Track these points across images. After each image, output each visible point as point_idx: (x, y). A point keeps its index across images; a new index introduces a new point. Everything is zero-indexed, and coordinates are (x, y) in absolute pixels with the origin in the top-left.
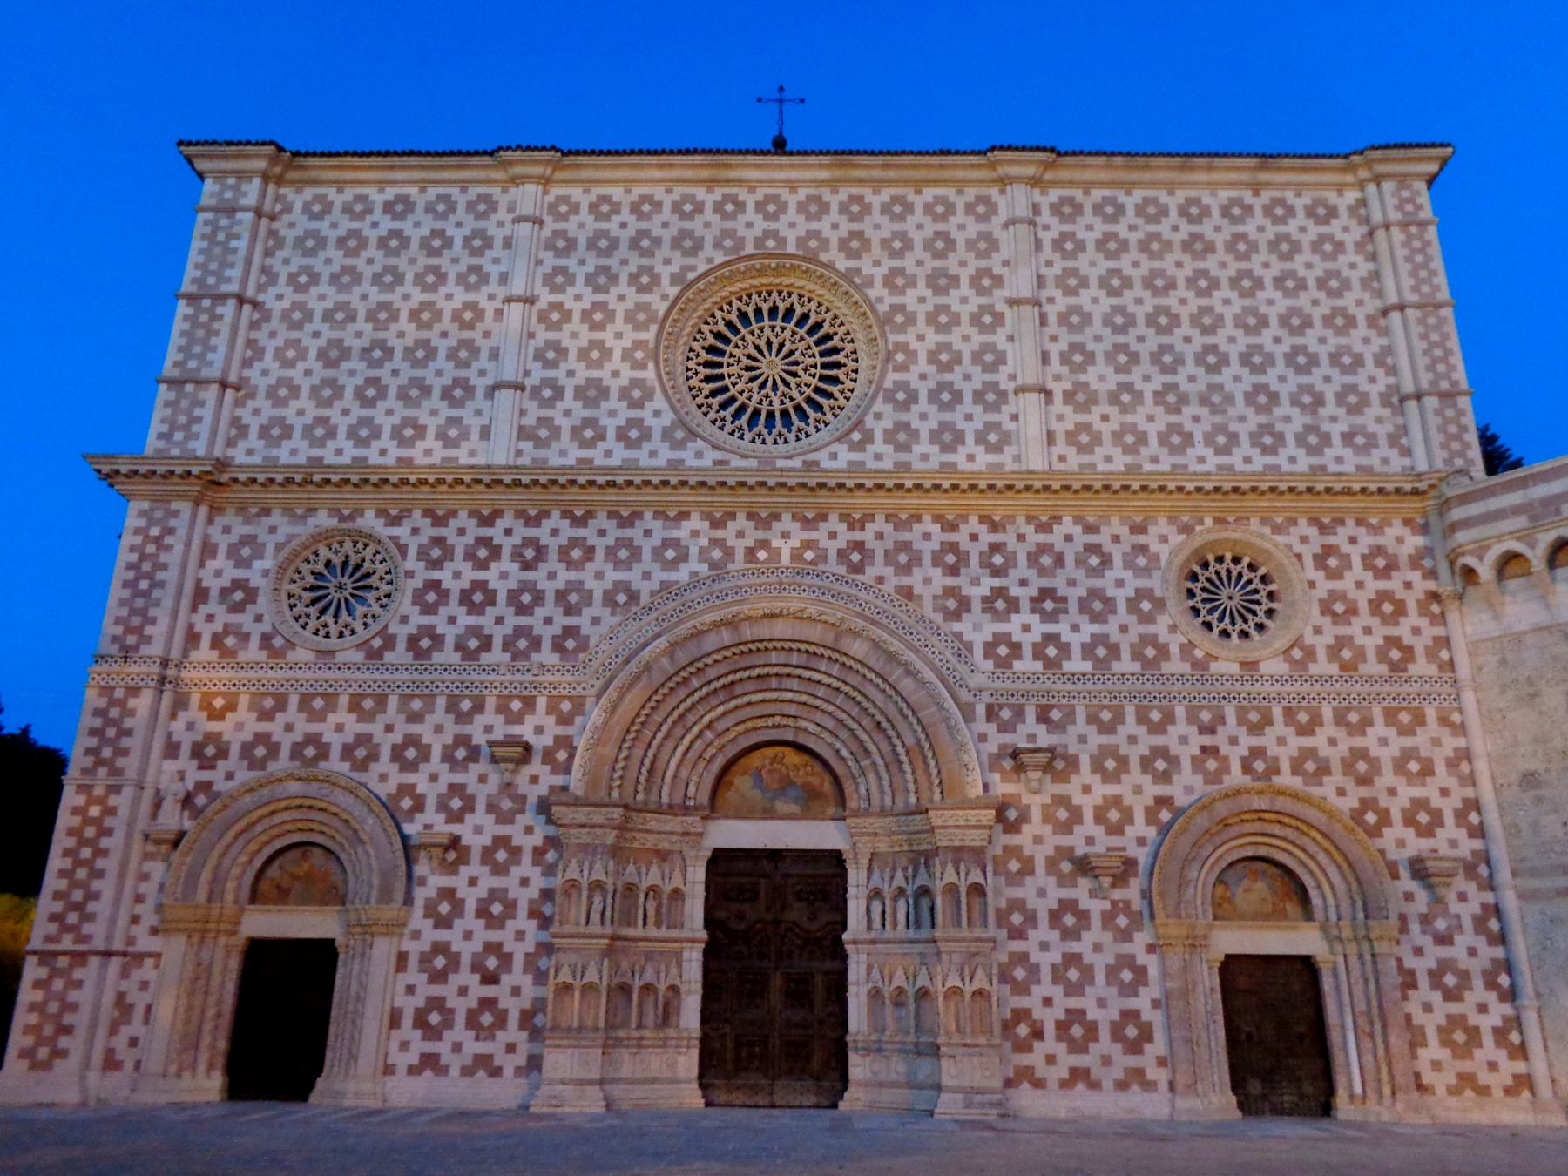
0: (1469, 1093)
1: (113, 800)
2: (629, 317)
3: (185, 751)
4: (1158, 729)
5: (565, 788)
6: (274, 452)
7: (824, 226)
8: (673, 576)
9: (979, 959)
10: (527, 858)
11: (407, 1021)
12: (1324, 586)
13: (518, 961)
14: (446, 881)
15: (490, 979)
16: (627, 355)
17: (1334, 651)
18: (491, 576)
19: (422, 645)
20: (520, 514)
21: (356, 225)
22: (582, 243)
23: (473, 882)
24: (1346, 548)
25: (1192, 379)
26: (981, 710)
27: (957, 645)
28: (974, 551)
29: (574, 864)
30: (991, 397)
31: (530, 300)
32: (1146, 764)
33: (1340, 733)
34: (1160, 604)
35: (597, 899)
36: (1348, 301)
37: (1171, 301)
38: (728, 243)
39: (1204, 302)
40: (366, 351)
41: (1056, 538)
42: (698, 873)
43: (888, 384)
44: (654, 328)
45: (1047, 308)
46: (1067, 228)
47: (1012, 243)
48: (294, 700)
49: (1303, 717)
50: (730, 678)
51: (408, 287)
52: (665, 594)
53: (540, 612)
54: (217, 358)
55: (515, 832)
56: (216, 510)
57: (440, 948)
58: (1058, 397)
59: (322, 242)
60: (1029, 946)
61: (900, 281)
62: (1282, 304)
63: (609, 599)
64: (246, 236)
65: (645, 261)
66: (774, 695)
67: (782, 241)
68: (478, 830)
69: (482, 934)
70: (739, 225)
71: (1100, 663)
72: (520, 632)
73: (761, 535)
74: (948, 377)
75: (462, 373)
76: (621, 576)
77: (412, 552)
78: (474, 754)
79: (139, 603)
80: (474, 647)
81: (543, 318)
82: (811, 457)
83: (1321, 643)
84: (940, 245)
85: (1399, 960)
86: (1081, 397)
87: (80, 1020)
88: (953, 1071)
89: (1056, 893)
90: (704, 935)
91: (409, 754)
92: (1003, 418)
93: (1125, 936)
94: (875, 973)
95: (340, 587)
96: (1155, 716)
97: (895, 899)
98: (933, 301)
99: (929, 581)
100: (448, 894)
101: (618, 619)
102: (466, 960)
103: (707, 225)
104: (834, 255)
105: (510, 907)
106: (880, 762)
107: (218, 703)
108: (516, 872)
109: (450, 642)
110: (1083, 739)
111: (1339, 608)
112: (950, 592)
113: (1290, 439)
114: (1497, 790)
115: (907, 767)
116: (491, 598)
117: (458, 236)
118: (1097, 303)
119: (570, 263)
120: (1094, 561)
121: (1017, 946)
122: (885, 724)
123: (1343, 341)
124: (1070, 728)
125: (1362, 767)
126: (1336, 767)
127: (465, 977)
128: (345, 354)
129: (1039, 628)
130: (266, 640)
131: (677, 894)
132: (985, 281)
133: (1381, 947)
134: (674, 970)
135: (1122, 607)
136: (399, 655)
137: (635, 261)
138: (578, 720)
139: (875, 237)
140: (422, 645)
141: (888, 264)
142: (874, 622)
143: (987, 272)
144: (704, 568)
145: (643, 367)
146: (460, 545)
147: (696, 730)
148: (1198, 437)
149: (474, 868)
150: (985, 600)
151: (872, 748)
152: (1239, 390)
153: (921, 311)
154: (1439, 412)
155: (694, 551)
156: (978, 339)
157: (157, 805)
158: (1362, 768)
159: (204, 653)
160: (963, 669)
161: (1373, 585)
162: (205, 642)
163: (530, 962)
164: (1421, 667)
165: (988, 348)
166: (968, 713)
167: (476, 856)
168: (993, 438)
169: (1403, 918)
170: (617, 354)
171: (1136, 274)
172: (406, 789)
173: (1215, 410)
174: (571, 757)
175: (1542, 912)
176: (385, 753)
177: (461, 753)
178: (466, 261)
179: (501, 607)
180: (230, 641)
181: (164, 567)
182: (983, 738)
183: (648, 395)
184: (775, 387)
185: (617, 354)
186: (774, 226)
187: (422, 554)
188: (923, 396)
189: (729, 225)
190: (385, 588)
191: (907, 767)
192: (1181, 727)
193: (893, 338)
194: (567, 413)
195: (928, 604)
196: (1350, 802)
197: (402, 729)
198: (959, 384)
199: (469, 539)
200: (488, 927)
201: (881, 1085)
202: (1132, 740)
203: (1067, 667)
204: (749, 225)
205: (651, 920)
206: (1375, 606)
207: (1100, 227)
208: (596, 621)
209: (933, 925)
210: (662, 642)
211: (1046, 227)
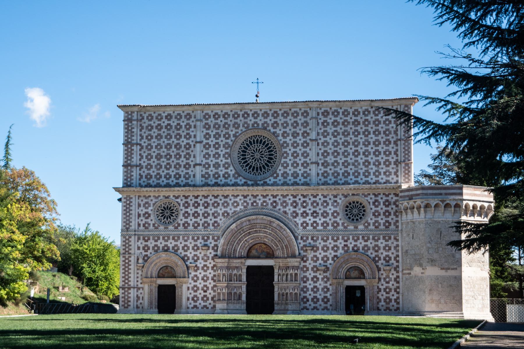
0: (388, 311)
1: (130, 259)
2: (224, 146)
3: (141, 248)
4: (335, 241)
5: (216, 255)
6: (149, 182)
7: (268, 120)
8: (236, 209)
10: (210, 269)
11: (190, 299)
12: (374, 209)
14: (195, 273)
15: (205, 291)
17: (374, 224)
18: (198, 210)
19: (186, 225)
21: (159, 122)
22: (212, 126)
23: (200, 273)
24: (380, 200)
25: (351, 159)
26: (300, 237)
28: (300, 202)
30: (305, 165)
31: (201, 142)
32: (333, 248)
33: (373, 242)
34: (338, 214)
36: (390, 137)
37: (348, 139)
38: (246, 125)
39: (356, 138)
40: (166, 156)
41: (317, 199)
42: (244, 271)
43: (282, 162)
44: (229, 148)
46: (325, 119)
47: (312, 123)
48: (161, 237)
49: (366, 238)
51: (173, 139)
53: (209, 218)
54: (134, 160)
55: (207, 263)
56: (139, 196)
57: (195, 286)
58: (320, 165)
59: (152, 127)
60: (307, 284)
61: (285, 135)
62: (374, 138)
63: (223, 214)
64: (136, 128)
67: (258, 125)
68: (200, 263)
69: (203, 283)
70: (248, 120)
71: (325, 227)
72: (205, 222)
73: (254, 200)
74: (296, 160)
75: (188, 161)
76: (225, 209)
77: (181, 205)
78: (198, 249)
79: (128, 218)
80: (196, 226)
81: (204, 146)
82: (266, 180)
83: (371, 222)
84: (295, 125)
85: (378, 287)
86: (325, 164)
87: (131, 300)
89: (313, 274)
90: (246, 283)
91: (186, 248)
92: (308, 170)
93: (326, 282)
95: (167, 213)
96: (335, 238)
98: (293, 140)
99: (290, 209)
100: (196, 276)
102: (200, 288)
103: (241, 121)
104: (270, 128)
105: (208, 278)
107: (146, 238)
108: (208, 271)
109: (191, 225)
110: (320, 243)
111: (377, 214)
112: (294, 212)
113: (372, 174)
114: (402, 253)
116: (199, 215)
117: (183, 125)
118: (330, 139)
119: (210, 132)
120: (325, 204)
121: (305, 284)
123: (387, 148)
125: (376, 248)
126: (371, 249)
127: (200, 291)
128: (161, 157)
129: (313, 220)
130: (154, 225)
132: (306, 134)
133: (375, 284)
135: (330, 215)
136: (181, 228)
137: (225, 131)
138: (218, 241)
139: (280, 123)
140: (186, 225)
141: (283, 130)
142: (278, 220)
143: (305, 132)
144: (242, 207)
145: (228, 159)
146: (191, 203)
148: (351, 174)
149: (200, 271)
150: (301, 213)
152: (361, 161)
153: (290, 143)
154: (404, 168)
155: (240, 204)
156: (303, 150)
157: (138, 259)
158: (376, 248)
159: (142, 228)
160: (296, 230)
161: (385, 209)
162: (142, 225)
163: (212, 288)
164: (392, 227)
165: (305, 152)
166: (296, 238)
167: (200, 268)
168: (305, 175)
169: (380, 279)
170: (222, 156)
171: (341, 131)
172: (186, 255)
173: (356, 167)
174: (218, 248)
176: (181, 248)
177: (196, 248)
178: (186, 132)
179: (201, 217)
180: (147, 225)
181: (131, 210)
182: (300, 243)
183: (229, 166)
184: (258, 161)
185: (222, 156)
186: (256, 120)
187: (184, 205)
189: (246, 120)
190: (176, 213)
192: (341, 240)
193: (284, 150)
194: (212, 171)
195: (289, 215)
196: (373, 255)
197: (184, 243)
198: (298, 162)
199: (193, 202)
202: (330, 243)
204: (251, 120)
206: (384, 214)
207: (333, 118)
208: (221, 220)
210: (234, 225)
211: (320, 119)
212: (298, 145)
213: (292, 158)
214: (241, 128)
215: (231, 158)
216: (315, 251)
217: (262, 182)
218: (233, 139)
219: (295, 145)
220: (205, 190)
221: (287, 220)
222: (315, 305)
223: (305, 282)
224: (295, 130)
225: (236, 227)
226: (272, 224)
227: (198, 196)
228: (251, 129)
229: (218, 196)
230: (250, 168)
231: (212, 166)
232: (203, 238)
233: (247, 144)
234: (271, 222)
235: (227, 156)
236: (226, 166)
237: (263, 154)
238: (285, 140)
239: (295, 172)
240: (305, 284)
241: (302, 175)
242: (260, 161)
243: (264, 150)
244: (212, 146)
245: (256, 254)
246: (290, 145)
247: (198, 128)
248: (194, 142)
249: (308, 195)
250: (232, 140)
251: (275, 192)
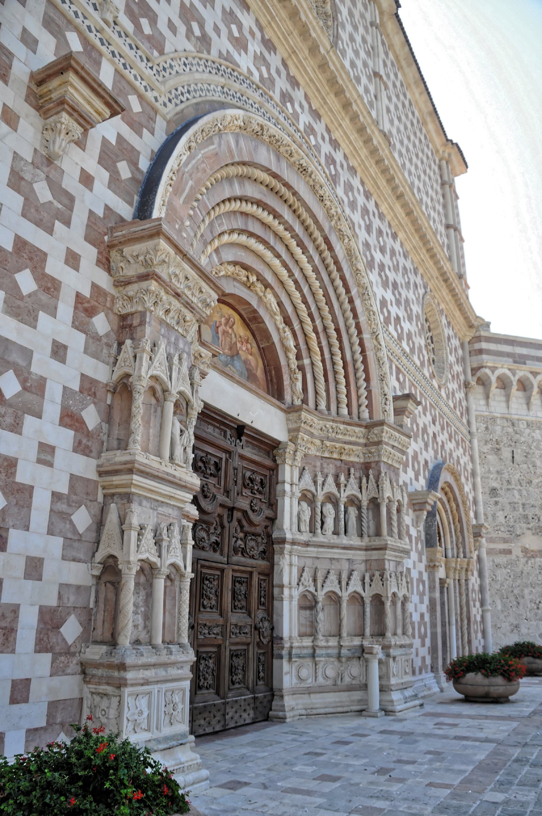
175: (493, 561)
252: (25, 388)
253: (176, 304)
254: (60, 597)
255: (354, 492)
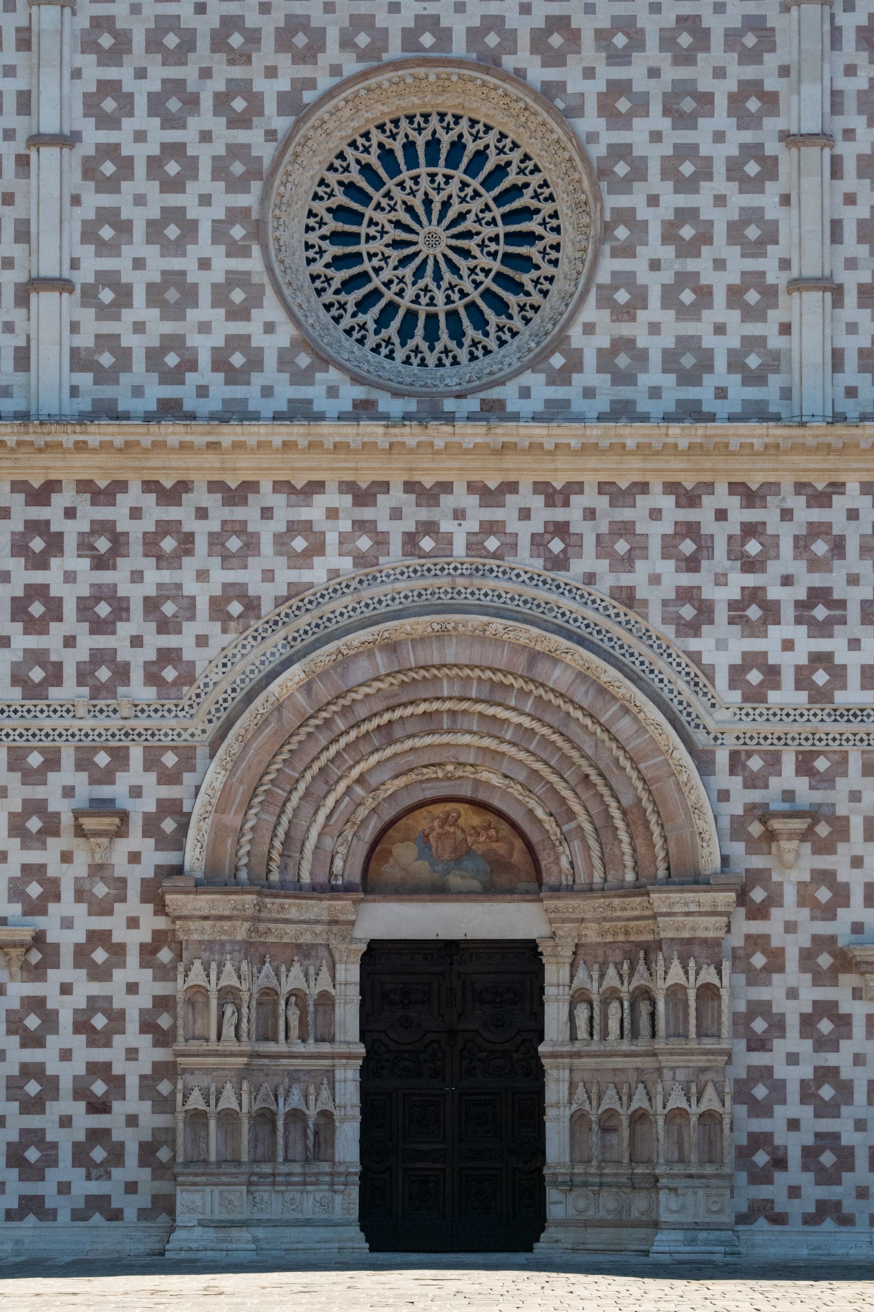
2: (219, 170)
5: (178, 870)
8: (304, 576)
9: (710, 1075)
10: (133, 958)
13: (132, 1085)
15: (98, 1107)
16: (219, 232)
20: (85, 486)
22: (139, 40)
23: (66, 989)
26: (722, 758)
27: (693, 669)
29: (197, 965)
30: (752, 297)
35: (229, 1009)
38: (363, 40)
43: (603, 277)
44: (256, 186)
45: (844, 148)
50: (387, 717)
52: (294, 602)
53: (125, 630)
58: (851, 297)
61: (623, 105)
63: (218, 608)
65: (237, 72)
66: (446, 739)
67: (444, 36)
68: (67, 923)
72: (99, 657)
73: (424, 514)
74: (691, 265)
76: (233, 576)
78: (52, 827)
81: (89, 170)
82: (495, 393)
84: (685, 40)
88: (673, 1206)
90: (361, 1049)
92: (769, 329)
94: (580, 1090)
97: (605, 1003)
98: (674, 137)
101: (231, 637)
102: (66, 1085)
105: (117, 1019)
106: (588, 827)
112: (686, 594)
115: (623, 836)
119: (124, 74)
121: (759, 1059)
122: (594, 778)
124: (840, 782)
131: (326, 1001)
134: (325, 1093)
138: (189, 778)
141: (606, 73)
142: (581, 641)
144: (346, 564)
147: (342, 787)
150: (733, 605)
151: (577, 808)
155: (332, 539)
156: (739, 200)
160: (699, 705)
163: (147, 1086)
167: (67, 956)
168: (753, 361)
170: (205, 231)
174: (183, 828)
177: (34, 824)
182: (724, 796)
183: (255, 300)
184: (438, 277)
185: (205, 231)
188: (655, 297)
191: (623, 836)
193: (613, 201)
194: (139, 327)
195: (655, 612)
200: (91, 1044)
201: (587, 1224)
203: (841, 698)
205: (294, 1032)
208: (202, 641)
209: (654, 1035)
210: (295, 674)
212: (705, 172)
213: (667, 252)
214: (332, 53)
215: (265, 248)
216: (825, 847)
217: (472, 404)
218: (282, 124)
219: (687, 169)
220: (105, 446)
221: (639, 647)
222: (824, 1192)
223: (759, 1044)
224: (683, 73)
225: (308, 688)
226: (542, 670)
227: (52, 487)
228: (397, 65)
229: (184, 486)
230: (382, 322)
231: (139, 296)
232: (84, 763)
233: (366, 169)
234: (534, 657)
235: (238, 232)
236: (238, 296)
237: (468, 235)
238: (619, 137)
239: (687, 343)
240: (759, 1059)
241: (736, 363)
242: (448, 276)
243: (476, 206)
244: (140, 168)
245: (422, 869)
246: (654, 169)
247: (48, 45)
248: (21, 137)
249: (773, 487)
250: (271, 135)
251: (562, 462)
252: (110, 1020)
253: (208, 924)
254: (153, 1135)
255: (643, 982)
